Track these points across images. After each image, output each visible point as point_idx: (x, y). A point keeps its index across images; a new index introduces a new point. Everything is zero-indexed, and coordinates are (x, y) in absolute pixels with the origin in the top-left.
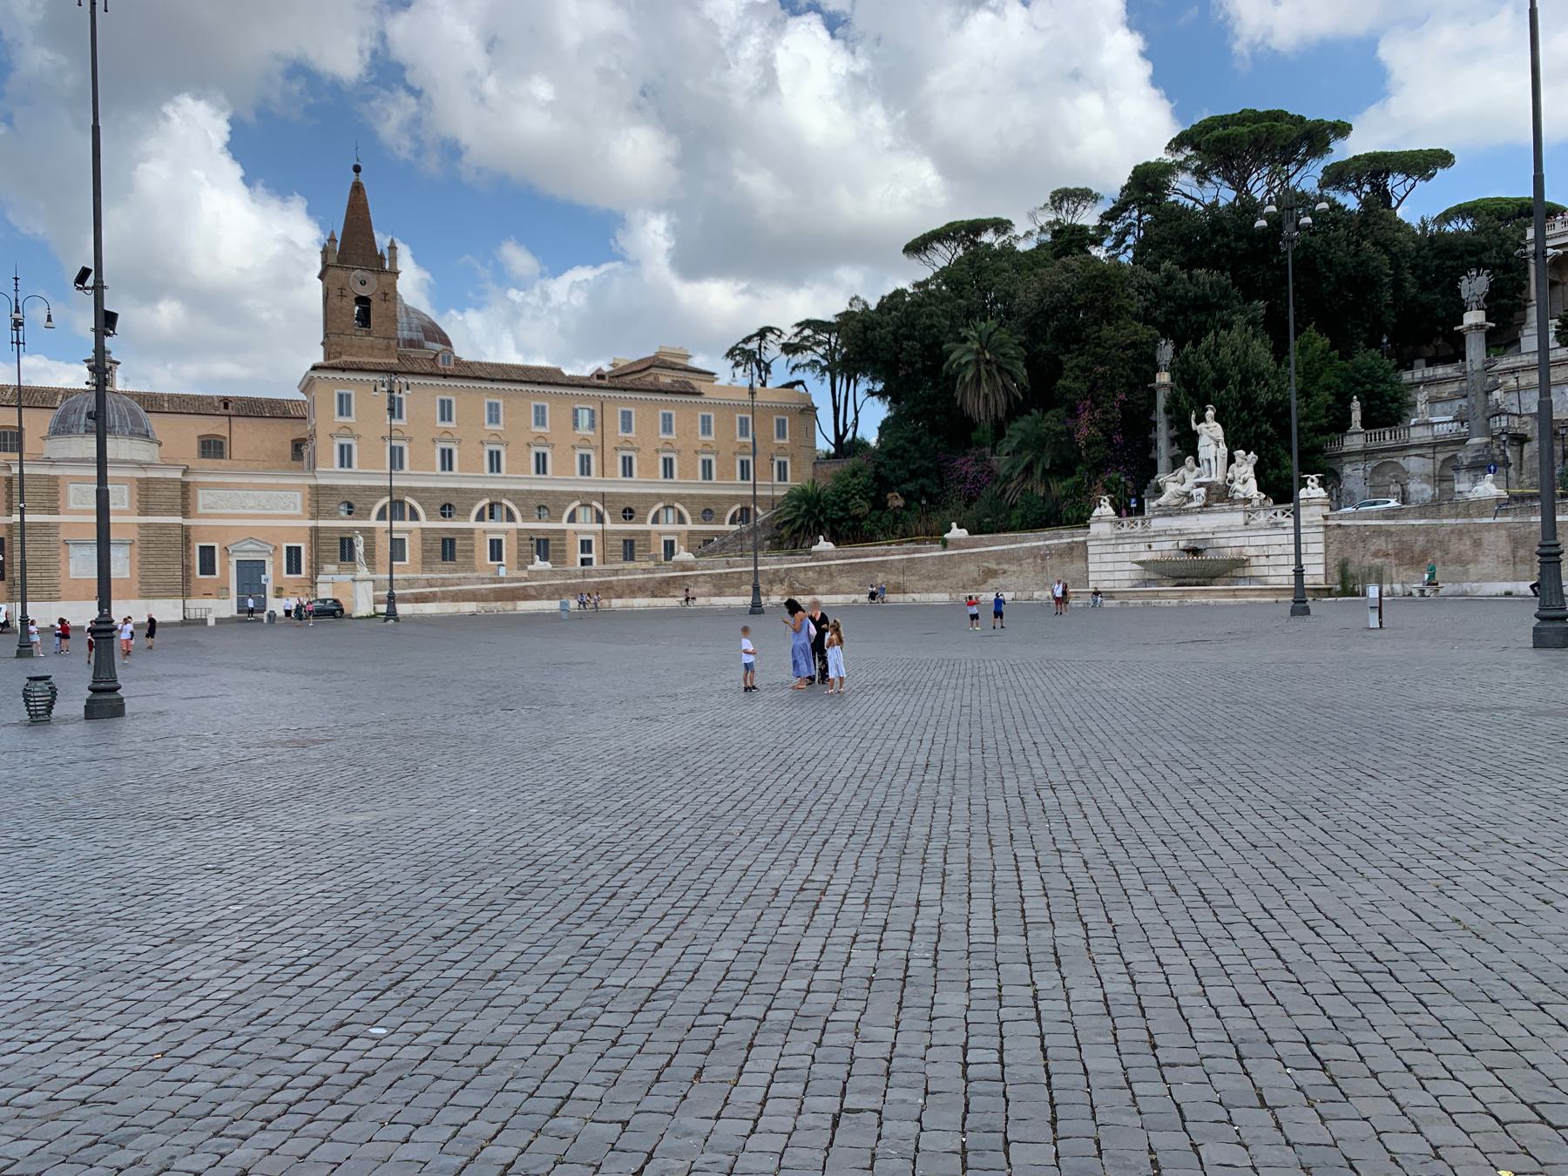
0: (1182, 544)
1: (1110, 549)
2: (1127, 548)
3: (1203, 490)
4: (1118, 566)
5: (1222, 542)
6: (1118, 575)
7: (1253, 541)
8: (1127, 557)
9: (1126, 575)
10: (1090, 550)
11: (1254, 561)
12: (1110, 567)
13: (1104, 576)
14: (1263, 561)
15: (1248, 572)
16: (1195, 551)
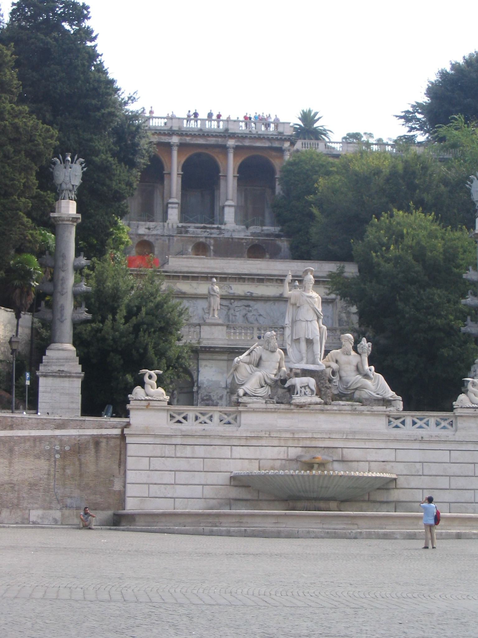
0: (293, 452)
1: (169, 451)
2: (200, 451)
3: (312, 382)
4: (182, 477)
5: (357, 454)
6: (181, 491)
7: (401, 456)
8: (197, 464)
9: (197, 491)
10: (131, 450)
11: (402, 482)
12: (168, 478)
13: (155, 490)
14: (415, 482)
15: (395, 495)
16: (322, 465)
